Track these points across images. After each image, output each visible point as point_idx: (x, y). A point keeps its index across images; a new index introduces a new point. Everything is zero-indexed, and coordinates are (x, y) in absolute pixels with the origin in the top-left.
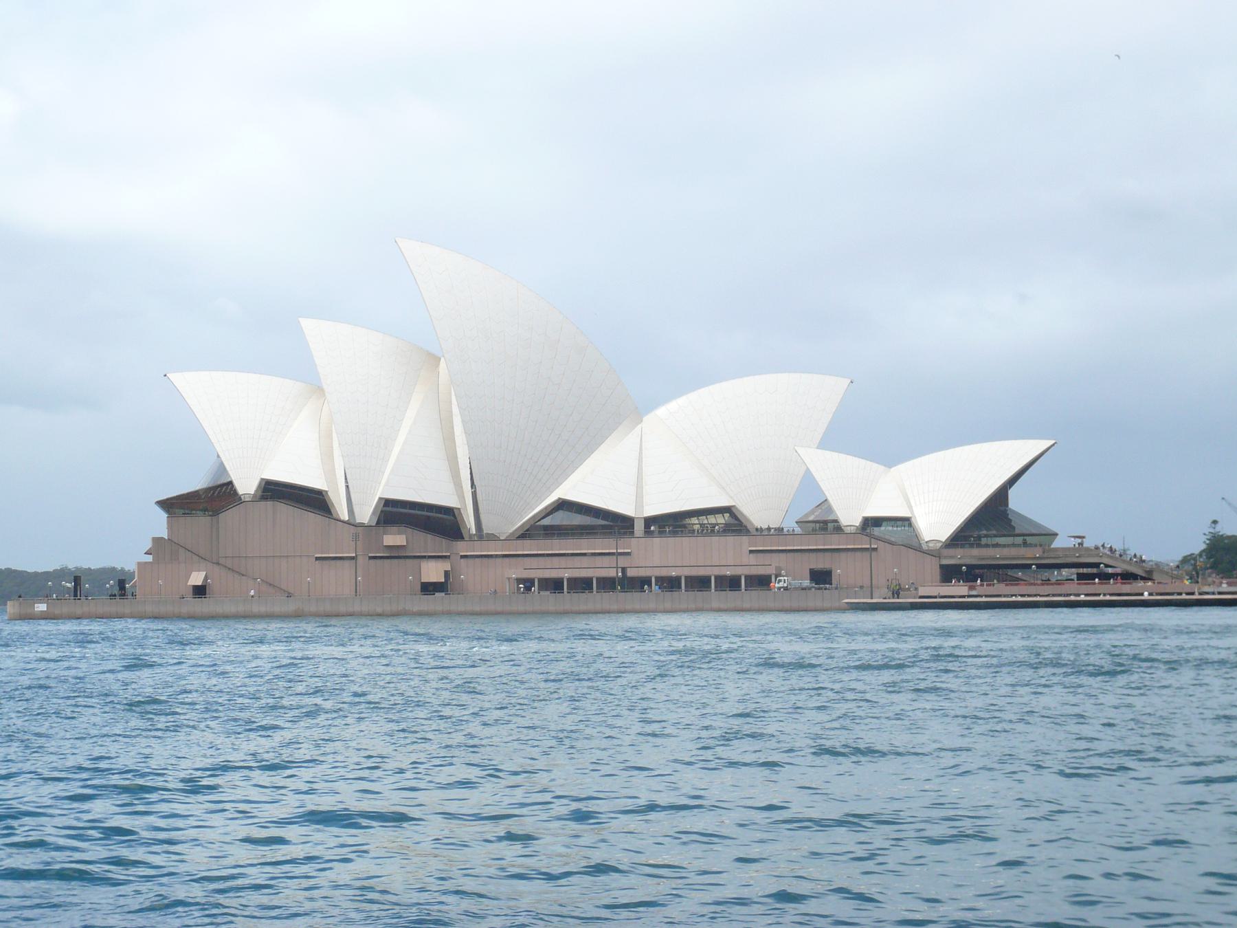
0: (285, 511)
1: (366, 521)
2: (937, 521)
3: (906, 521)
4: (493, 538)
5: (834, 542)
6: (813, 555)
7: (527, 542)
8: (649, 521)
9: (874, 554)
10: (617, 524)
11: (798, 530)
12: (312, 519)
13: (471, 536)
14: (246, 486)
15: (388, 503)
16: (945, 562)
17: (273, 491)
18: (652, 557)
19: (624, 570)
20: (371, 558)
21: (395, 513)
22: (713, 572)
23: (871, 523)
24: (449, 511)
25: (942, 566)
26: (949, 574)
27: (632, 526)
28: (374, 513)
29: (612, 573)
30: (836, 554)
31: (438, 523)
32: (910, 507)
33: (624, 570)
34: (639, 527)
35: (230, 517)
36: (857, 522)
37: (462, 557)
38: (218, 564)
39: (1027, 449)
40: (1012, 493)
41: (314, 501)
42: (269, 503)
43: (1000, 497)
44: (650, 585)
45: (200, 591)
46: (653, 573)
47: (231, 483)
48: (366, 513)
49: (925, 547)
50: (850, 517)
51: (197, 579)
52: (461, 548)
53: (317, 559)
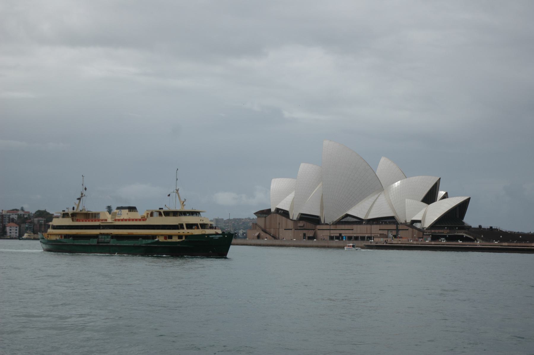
3: (419, 221)
4: (327, 224)
12: (284, 218)
14: (273, 210)
15: (302, 214)
17: (278, 210)
18: (359, 230)
24: (318, 217)
33: (340, 234)
35: (268, 217)
41: (285, 214)
51: (257, 234)
52: (318, 227)
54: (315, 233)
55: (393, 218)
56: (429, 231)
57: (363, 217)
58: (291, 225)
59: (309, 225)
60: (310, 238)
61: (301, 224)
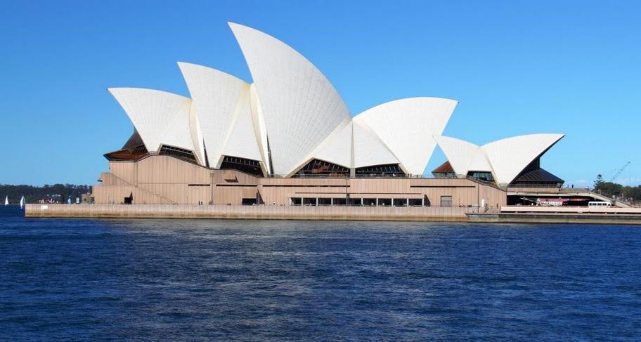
0: (173, 161)
1: (215, 167)
3: (490, 173)
5: (453, 182)
7: (297, 179)
8: (357, 169)
10: (342, 171)
11: (433, 177)
13: (268, 175)
15: (226, 157)
16: (509, 194)
17: (167, 151)
19: (348, 195)
21: (229, 163)
22: (392, 197)
23: (470, 173)
24: (257, 162)
25: (508, 196)
26: (512, 200)
27: (349, 173)
28: (219, 163)
29: (344, 196)
30: (454, 189)
31: (252, 168)
32: (491, 166)
33: (348, 195)
34: (353, 173)
35: (143, 163)
36: (465, 173)
37: (264, 186)
38: (137, 186)
39: (550, 138)
40: (541, 158)
41: (186, 155)
42: (165, 157)
43: (536, 163)
44: (375, 204)
45: (128, 201)
46: (362, 197)
47: (144, 146)
48: (215, 162)
49: (498, 185)
50: (461, 169)
52: (263, 181)
54: (259, 195)
55: (396, 165)
56: (517, 189)
57: (346, 164)
58: (205, 177)
59: (243, 178)
60: (247, 202)
61: (230, 174)
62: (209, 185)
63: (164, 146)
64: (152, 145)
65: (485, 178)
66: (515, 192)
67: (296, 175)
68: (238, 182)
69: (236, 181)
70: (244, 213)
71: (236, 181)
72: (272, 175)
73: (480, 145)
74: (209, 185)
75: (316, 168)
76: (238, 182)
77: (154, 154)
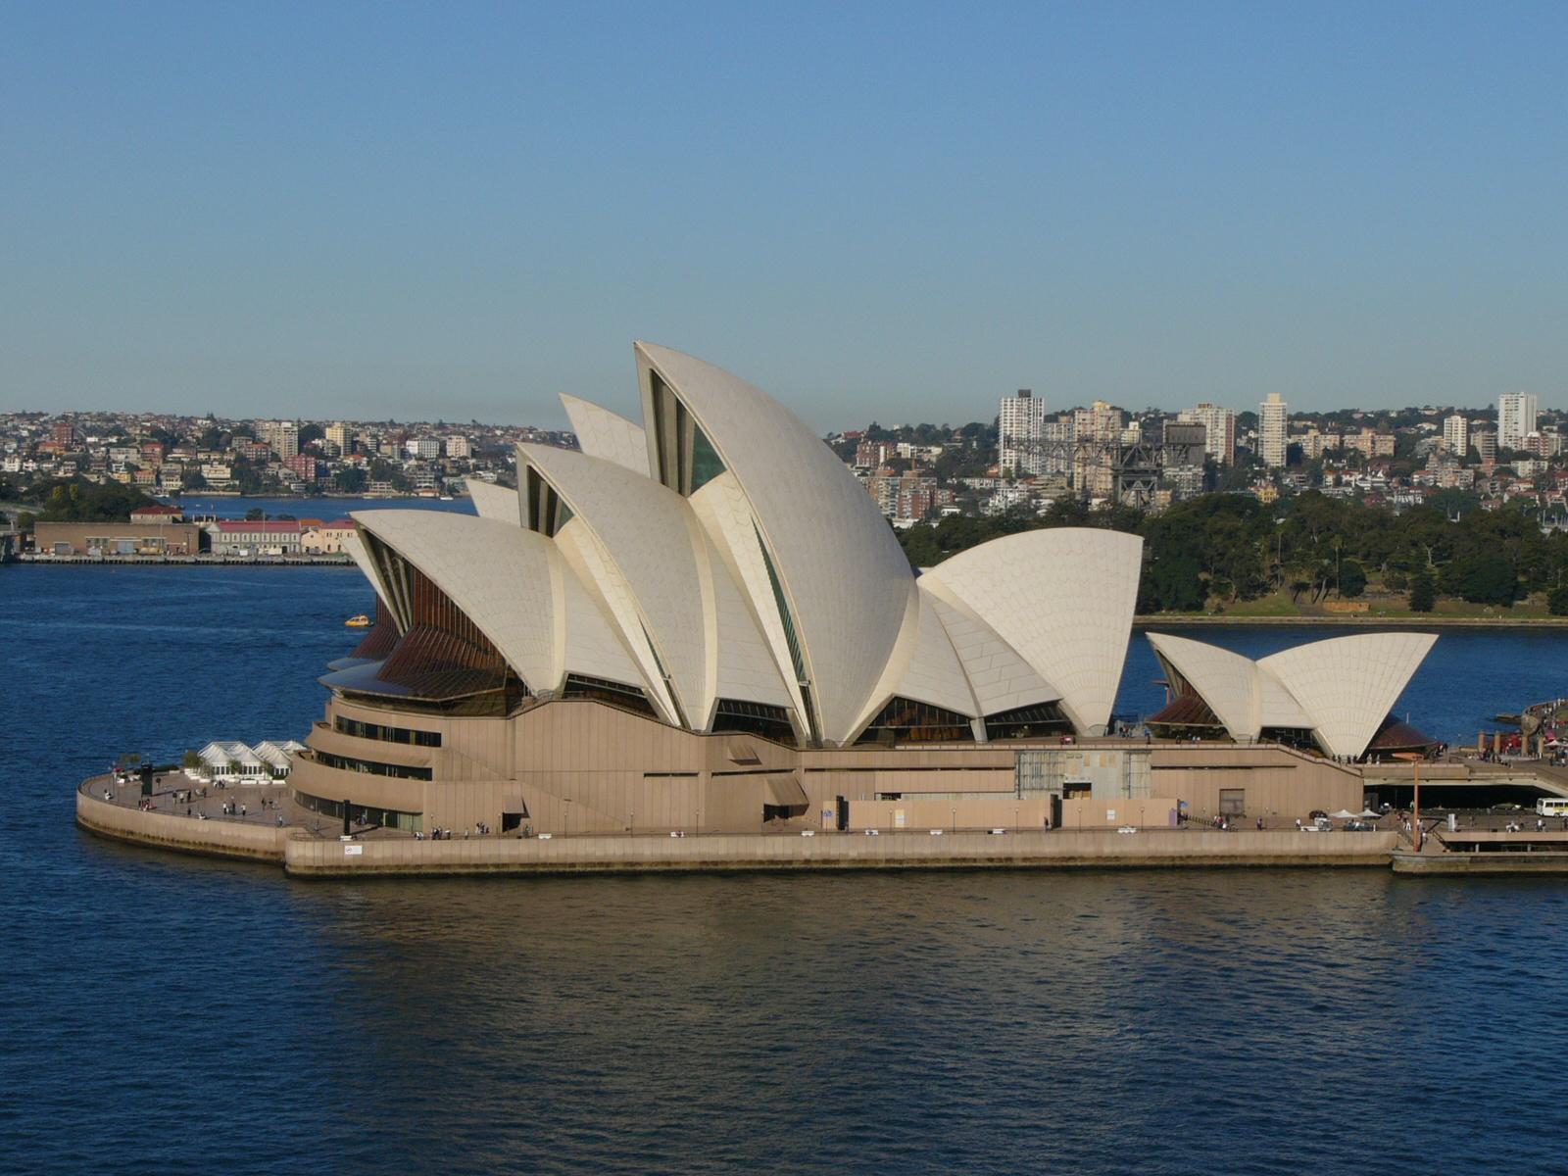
2: (1348, 729)
4: (831, 747)
6: (1225, 773)
8: (988, 719)
9: (1291, 772)
15: (724, 705)
17: (578, 687)
20: (713, 774)
21: (732, 716)
23: (1269, 734)
25: (1368, 789)
34: (978, 730)
35: (526, 722)
36: (1255, 732)
41: (631, 700)
45: (510, 822)
48: (702, 717)
52: (808, 759)
53: (646, 775)
55: (1054, 704)
58: (688, 753)
59: (769, 752)
62: (695, 775)
63: (571, 676)
64: (543, 674)
65: (1302, 739)
66: (1382, 774)
67: (868, 737)
68: (760, 763)
69: (757, 762)
70: (853, 854)
71: (757, 762)
72: (816, 743)
73: (1255, 660)
74: (695, 775)
75: (906, 723)
76: (760, 763)
77: (547, 699)
